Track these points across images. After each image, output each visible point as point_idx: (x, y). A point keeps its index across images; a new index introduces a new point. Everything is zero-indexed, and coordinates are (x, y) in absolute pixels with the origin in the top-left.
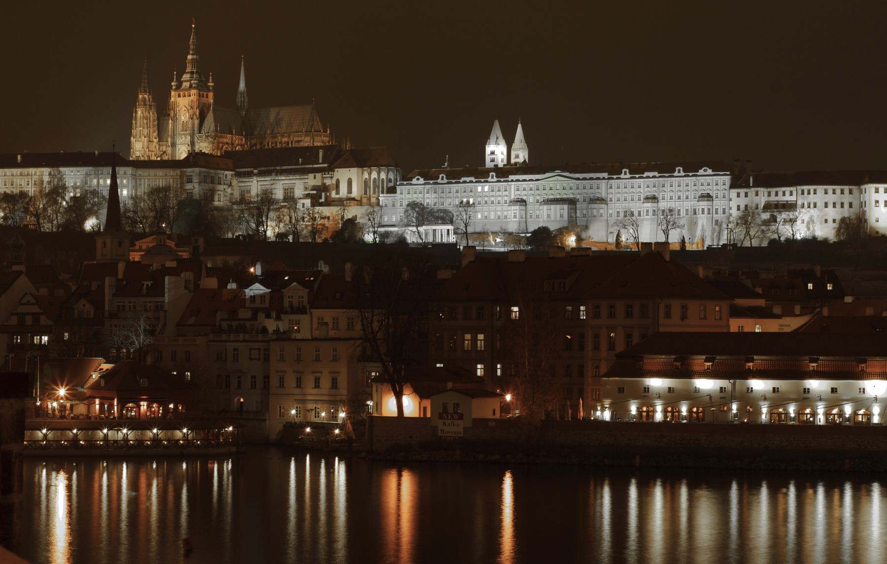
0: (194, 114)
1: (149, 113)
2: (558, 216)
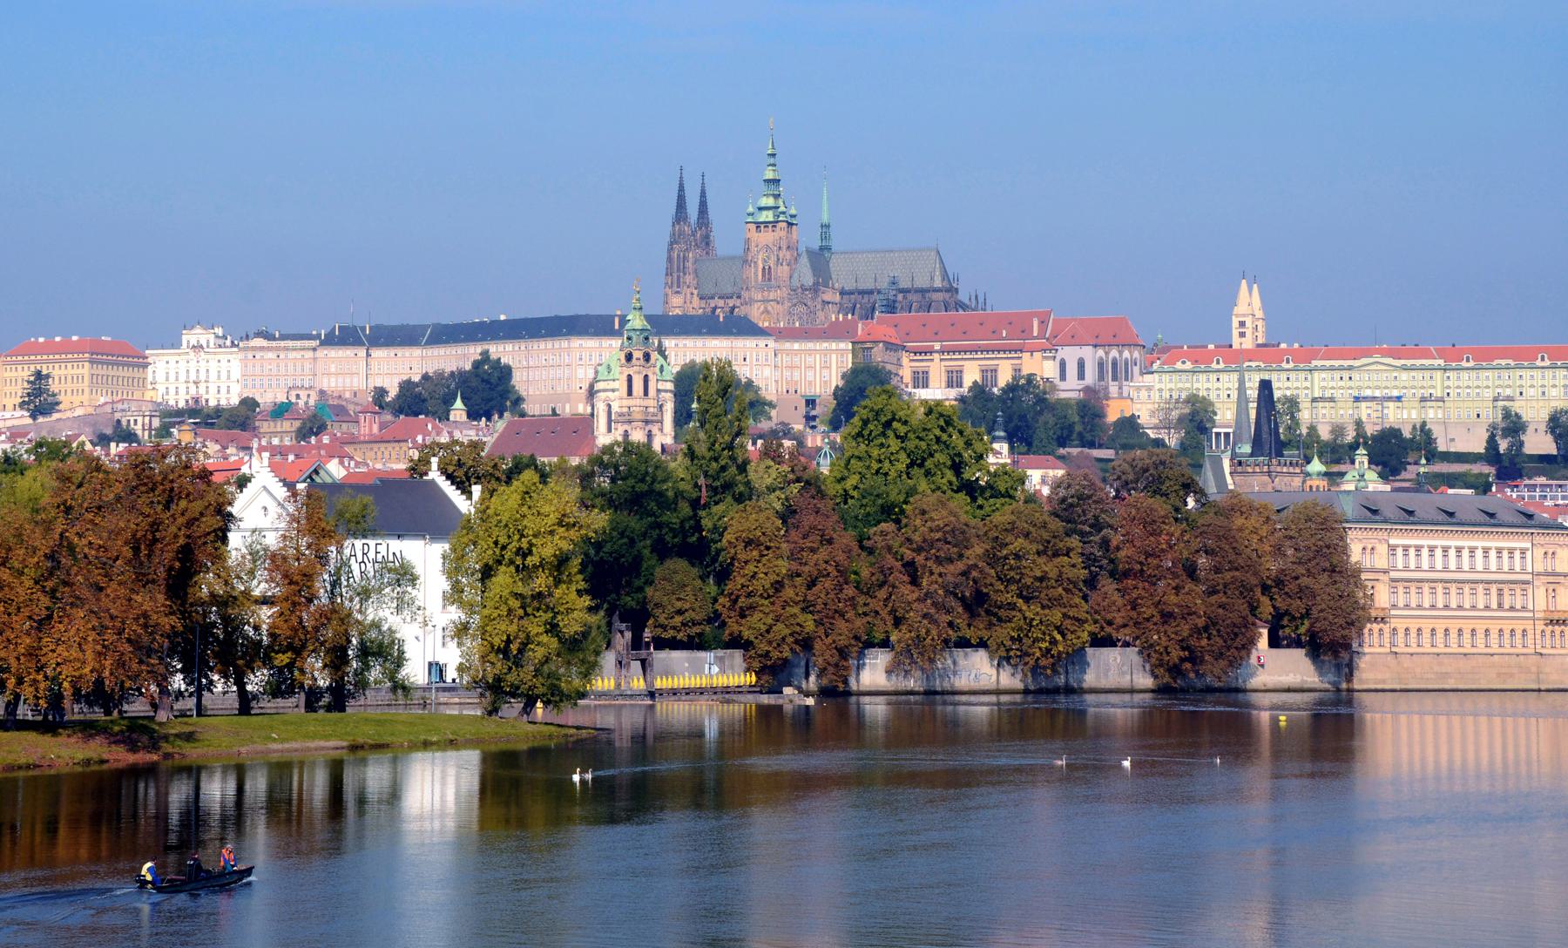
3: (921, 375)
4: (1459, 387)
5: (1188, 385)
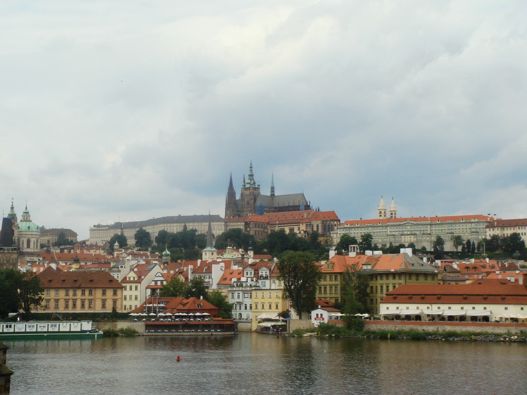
3: (273, 231)
4: (435, 230)
5: (348, 232)
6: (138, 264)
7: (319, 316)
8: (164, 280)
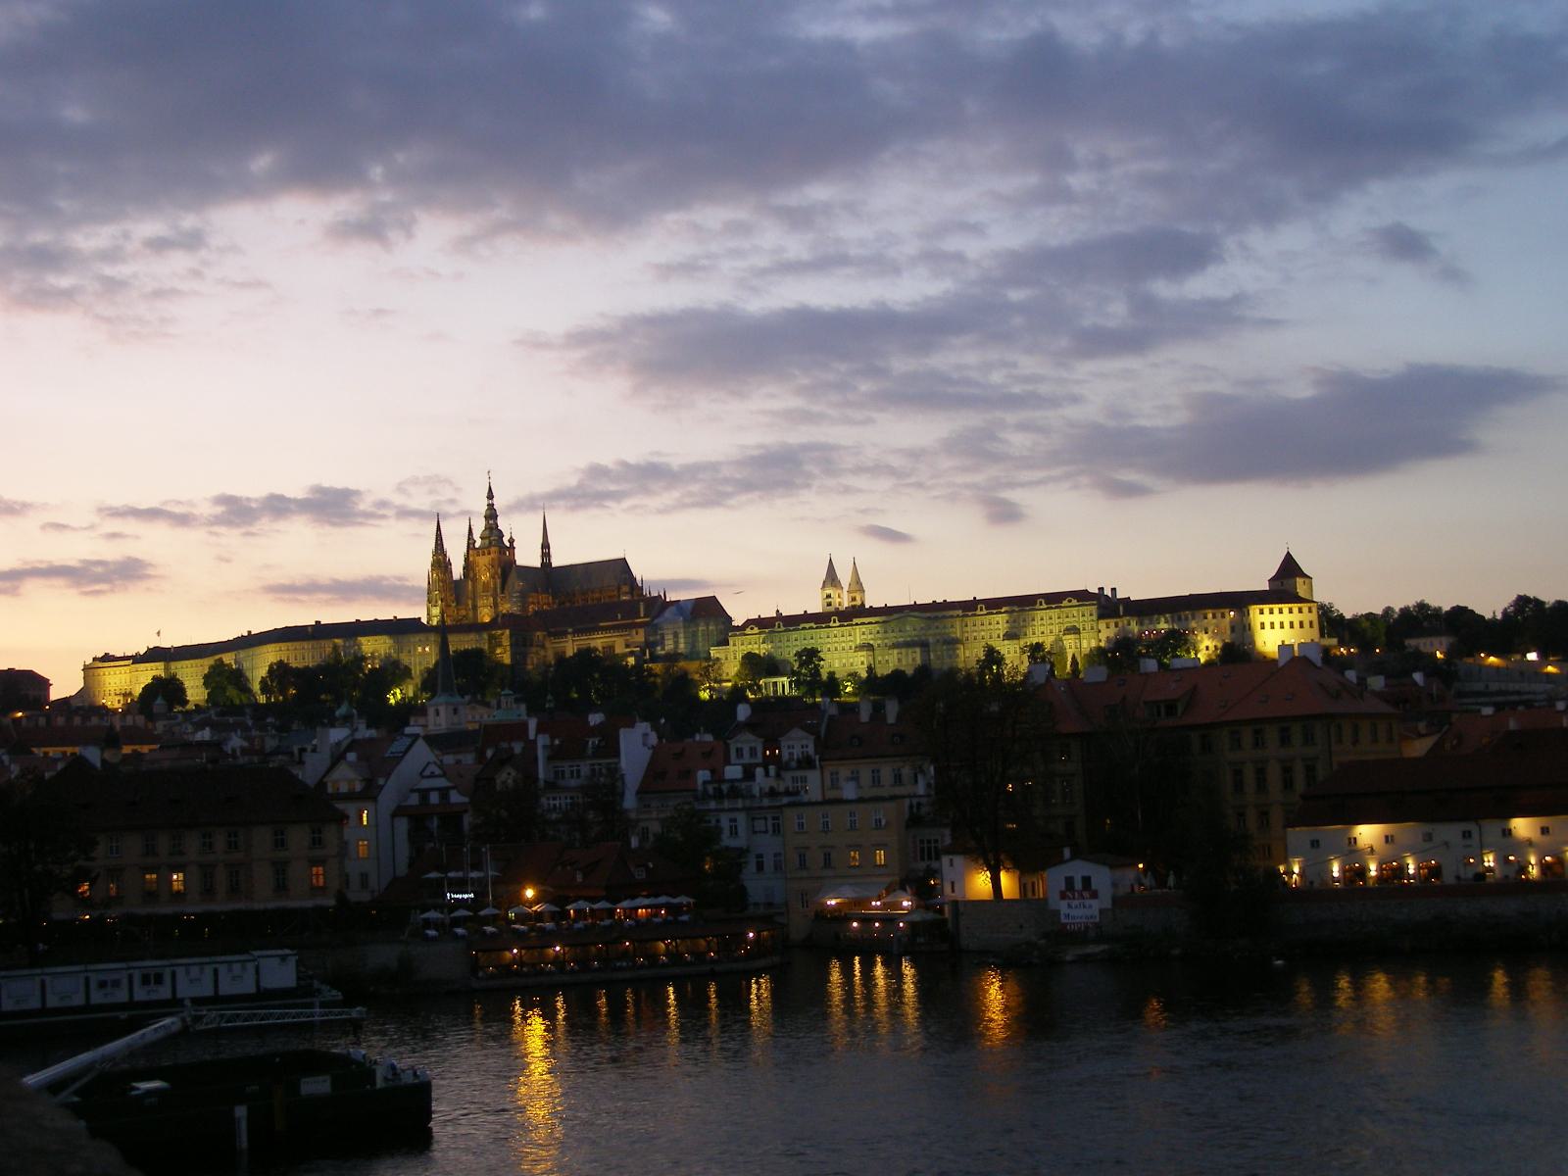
0: (496, 573)
1: (444, 575)
2: (910, 660)
6: (354, 741)
7: (1078, 885)
8: (453, 788)
